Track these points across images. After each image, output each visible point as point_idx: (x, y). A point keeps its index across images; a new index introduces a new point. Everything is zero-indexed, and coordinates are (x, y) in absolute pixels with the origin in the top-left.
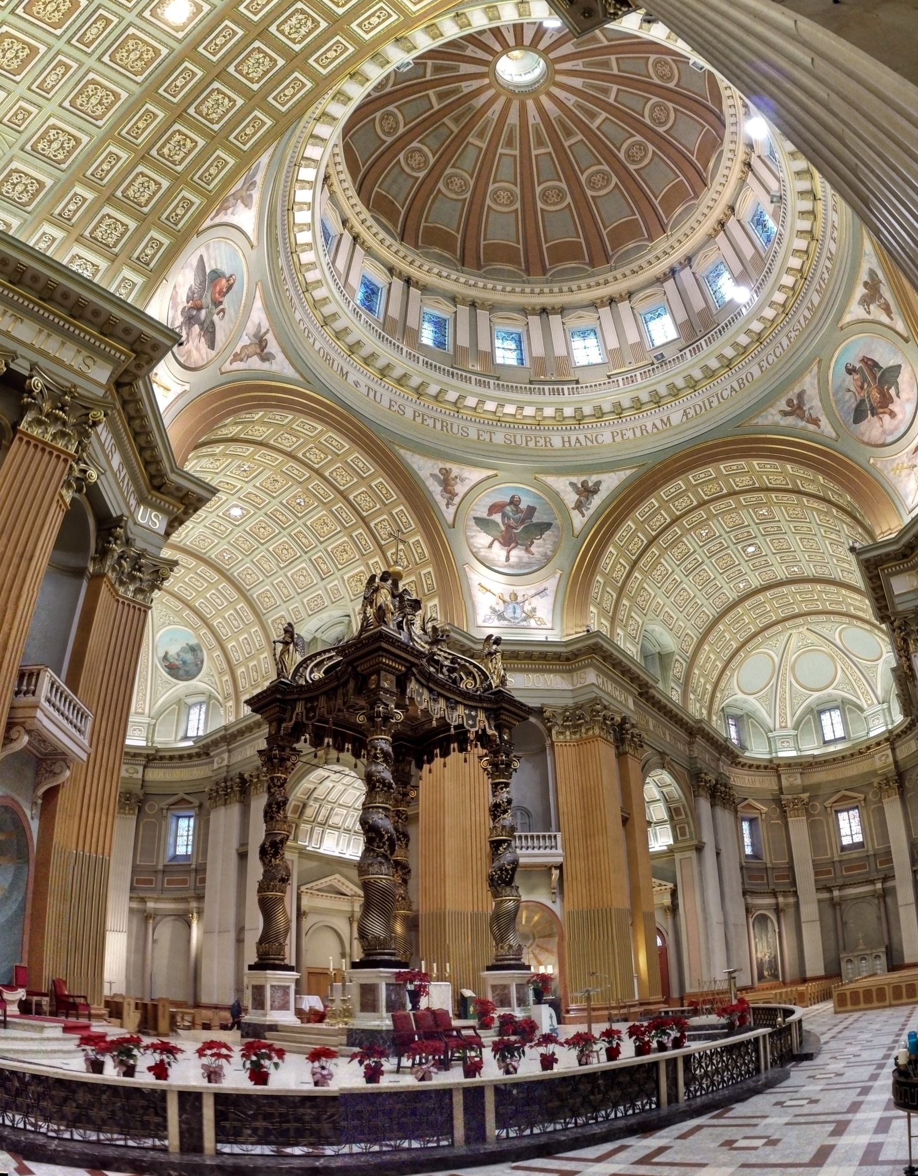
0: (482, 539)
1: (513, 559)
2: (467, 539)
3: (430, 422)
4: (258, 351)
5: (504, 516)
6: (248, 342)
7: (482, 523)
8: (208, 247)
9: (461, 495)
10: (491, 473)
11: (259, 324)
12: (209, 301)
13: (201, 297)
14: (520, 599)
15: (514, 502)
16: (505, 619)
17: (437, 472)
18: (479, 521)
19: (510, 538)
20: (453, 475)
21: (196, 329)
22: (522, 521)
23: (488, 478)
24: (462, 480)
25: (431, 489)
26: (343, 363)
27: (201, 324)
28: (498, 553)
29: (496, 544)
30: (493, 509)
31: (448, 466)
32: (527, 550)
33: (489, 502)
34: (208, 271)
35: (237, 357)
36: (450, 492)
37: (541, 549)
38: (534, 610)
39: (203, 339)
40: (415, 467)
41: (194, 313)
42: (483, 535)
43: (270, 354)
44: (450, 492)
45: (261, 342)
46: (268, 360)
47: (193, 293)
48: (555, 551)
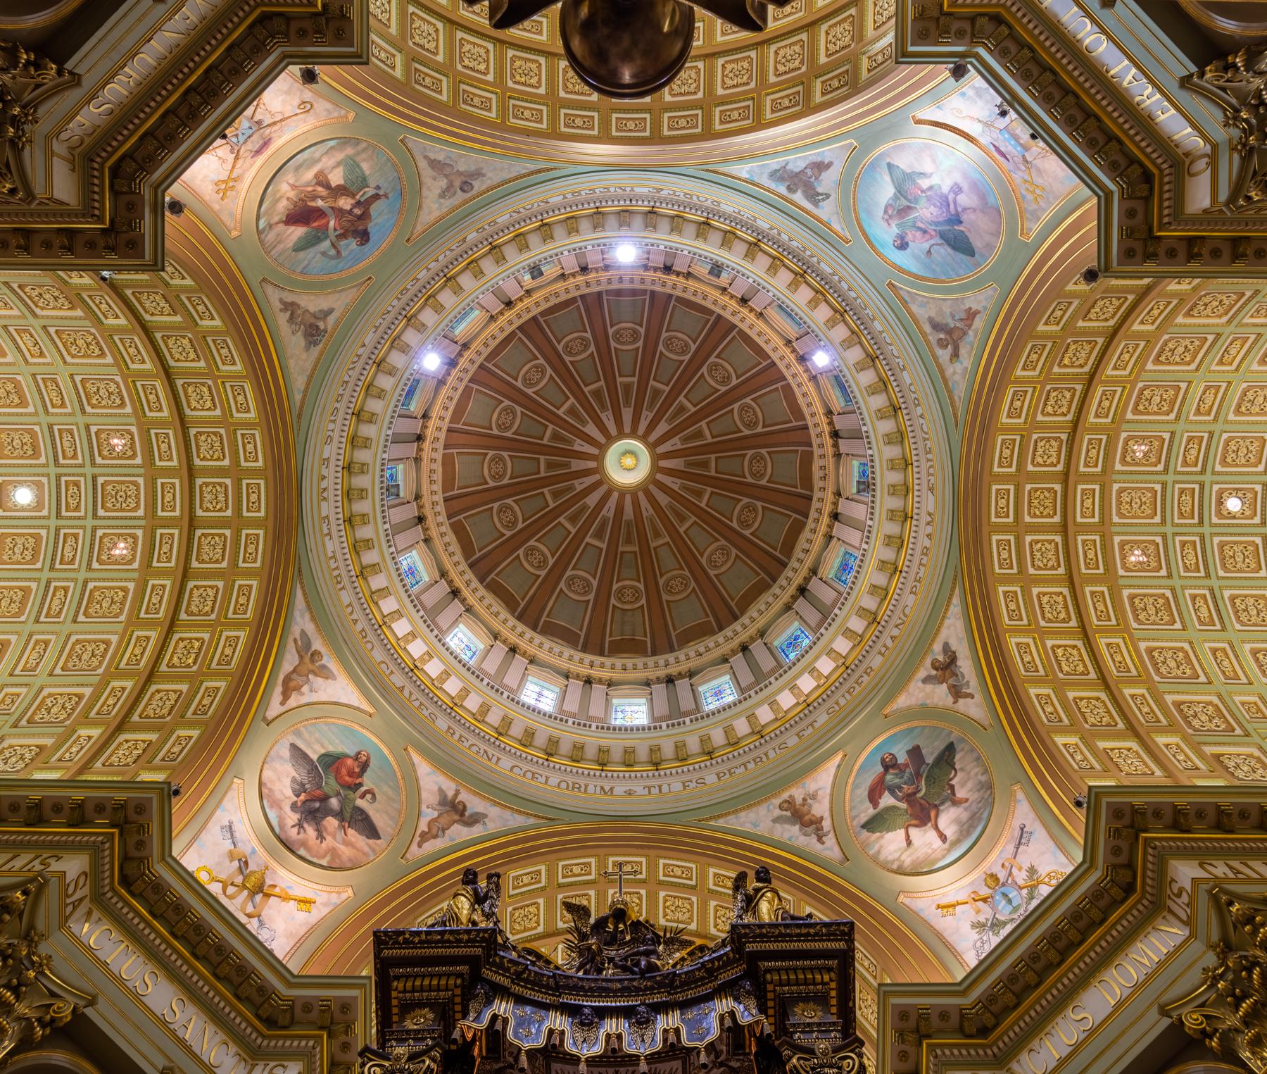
0: (891, 843)
1: (950, 832)
2: (875, 859)
5: (892, 791)
6: (436, 814)
7: (875, 824)
8: (298, 734)
9: (827, 815)
12: (338, 787)
13: (319, 786)
14: (1002, 875)
15: (889, 764)
16: (1004, 924)
17: (777, 812)
18: (871, 825)
19: (922, 808)
20: (799, 800)
21: (331, 823)
22: (918, 775)
24: (814, 796)
26: (599, 783)
27: (339, 815)
28: (925, 839)
29: (913, 831)
30: (874, 796)
32: (956, 803)
33: (863, 792)
34: (314, 757)
37: (970, 785)
38: (1032, 871)
39: (351, 831)
41: (317, 805)
42: (889, 836)
44: (811, 823)
48: (986, 771)
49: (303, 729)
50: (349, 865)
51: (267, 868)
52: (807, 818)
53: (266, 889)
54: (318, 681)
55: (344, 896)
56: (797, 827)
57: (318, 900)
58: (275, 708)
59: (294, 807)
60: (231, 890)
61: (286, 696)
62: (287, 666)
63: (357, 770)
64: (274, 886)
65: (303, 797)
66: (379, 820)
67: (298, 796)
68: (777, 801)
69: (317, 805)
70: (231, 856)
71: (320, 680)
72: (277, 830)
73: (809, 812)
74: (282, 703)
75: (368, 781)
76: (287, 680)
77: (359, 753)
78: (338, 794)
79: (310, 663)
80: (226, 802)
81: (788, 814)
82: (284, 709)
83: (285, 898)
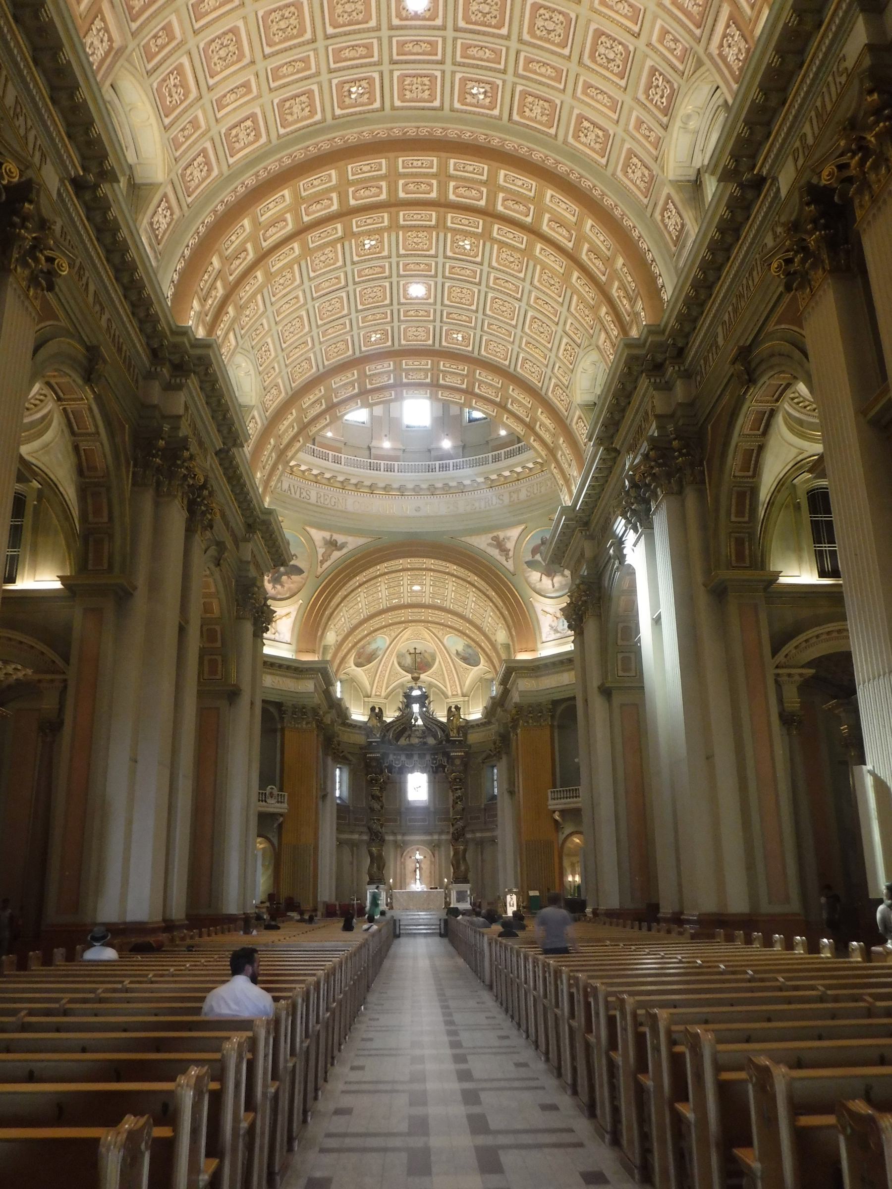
0: (535, 576)
1: (556, 585)
7: (531, 564)
9: (512, 549)
11: (324, 538)
16: (558, 632)
17: (490, 541)
20: (501, 538)
21: (284, 578)
23: (523, 530)
24: (509, 539)
27: (286, 574)
28: (546, 582)
29: (544, 577)
32: (563, 575)
33: (531, 547)
35: (322, 562)
36: (505, 551)
39: (293, 577)
40: (475, 544)
42: (534, 573)
44: (505, 551)
45: (332, 545)
56: (498, 551)
68: (491, 535)
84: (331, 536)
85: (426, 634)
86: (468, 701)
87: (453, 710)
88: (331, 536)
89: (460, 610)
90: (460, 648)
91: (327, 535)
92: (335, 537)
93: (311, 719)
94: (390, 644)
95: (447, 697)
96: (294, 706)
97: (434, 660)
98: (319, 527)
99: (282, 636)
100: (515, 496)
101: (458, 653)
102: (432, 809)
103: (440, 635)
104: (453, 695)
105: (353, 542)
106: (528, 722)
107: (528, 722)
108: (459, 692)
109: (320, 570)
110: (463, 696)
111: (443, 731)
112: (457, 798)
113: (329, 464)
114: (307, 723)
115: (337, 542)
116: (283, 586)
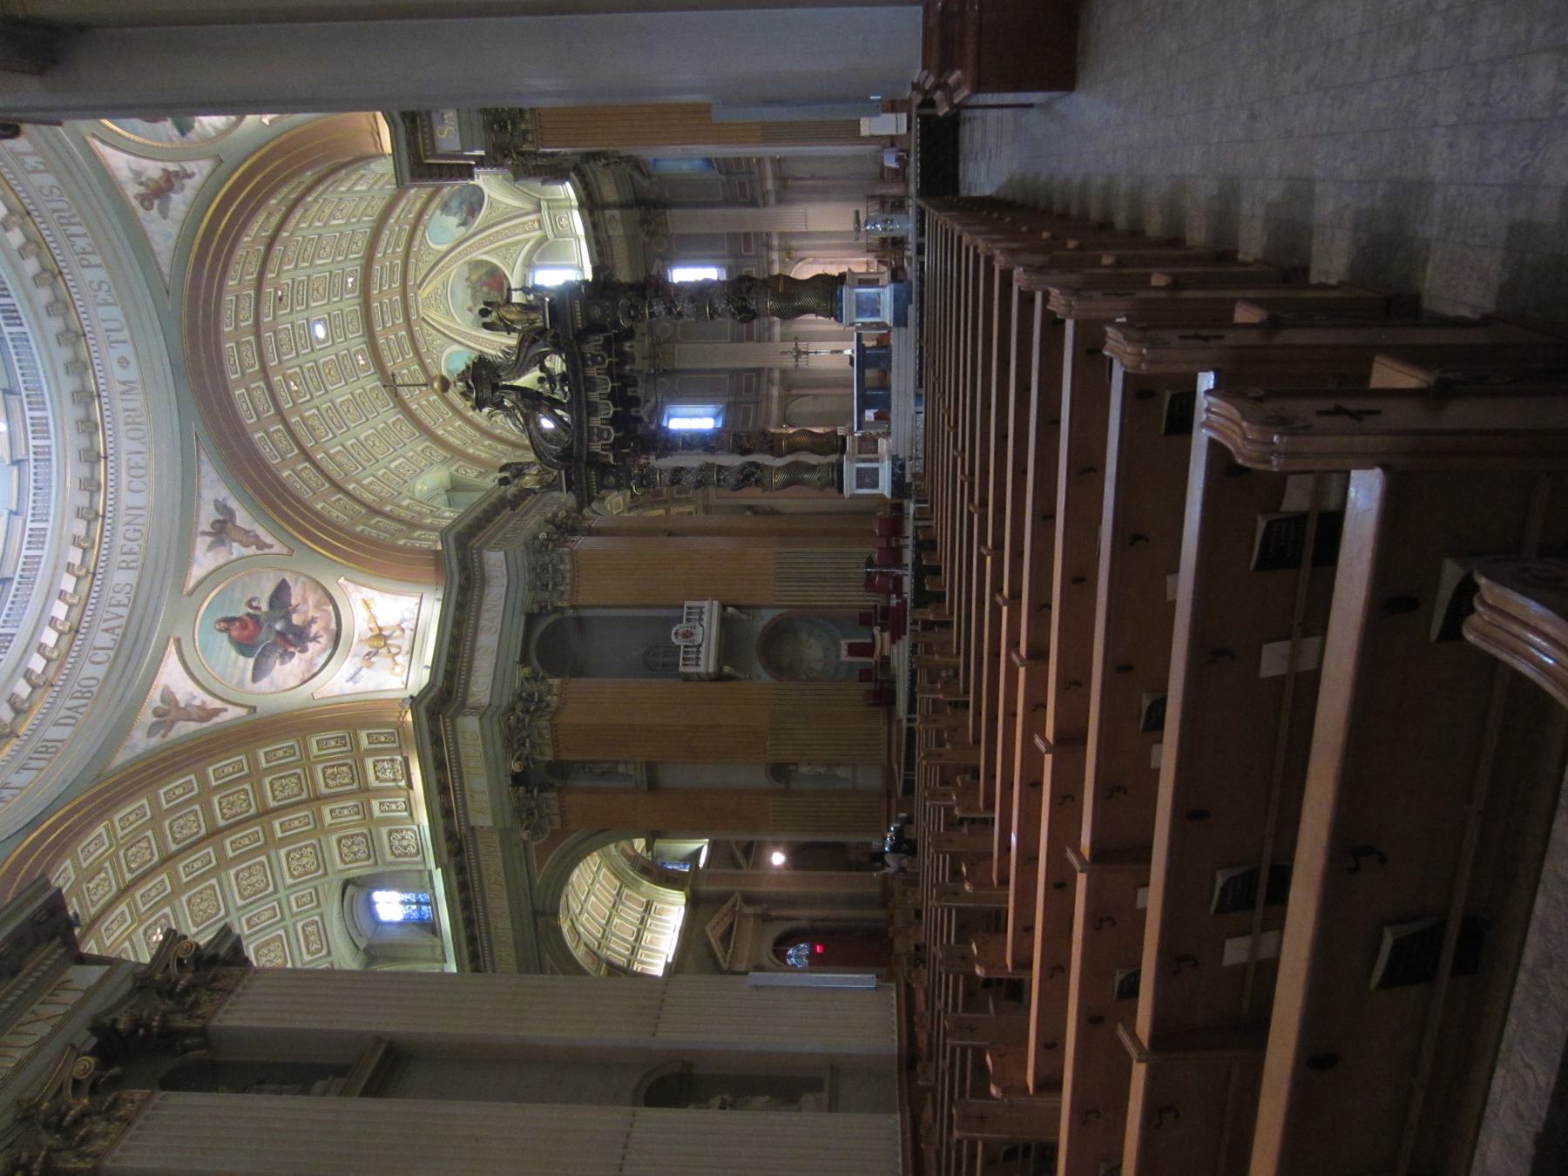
3: (81, 243)
4: (230, 526)
8: (241, 683)
9: (161, 165)
10: (97, 144)
11: (211, 547)
13: (274, 644)
17: (155, 212)
20: (142, 190)
21: (296, 619)
23: (103, 142)
24: (137, 174)
25: (183, 208)
27: (287, 617)
31: (135, 203)
34: (251, 661)
35: (261, 545)
39: (294, 602)
40: (171, 243)
41: (290, 636)
43: (217, 509)
46: (225, 507)
47: (282, 656)
49: (234, 682)
50: (320, 591)
51: (360, 641)
52: (163, 184)
53: (377, 632)
54: (182, 699)
55: (346, 583)
57: (359, 597)
58: (233, 713)
59: (304, 650)
60: (394, 650)
61: (216, 712)
62: (192, 727)
63: (238, 624)
64: (371, 629)
65: (292, 649)
66: (268, 588)
67: (293, 654)
68: (141, 212)
69: (290, 636)
70: (370, 665)
71: (178, 697)
72: (329, 651)
73: (156, 182)
74: (225, 710)
75: (242, 610)
76: (202, 720)
77: (220, 630)
78: (270, 627)
79: (170, 711)
80: (337, 692)
81: (156, 202)
82: (229, 707)
83: (374, 618)
84: (204, 533)
85: (424, 293)
86: (548, 201)
87: (488, 320)
88: (204, 533)
89: (361, 242)
90: (452, 221)
91: (202, 543)
92: (205, 525)
93: (554, 555)
94: (459, 342)
95: (545, 239)
96: (532, 587)
97: (481, 262)
98: (185, 559)
99: (407, 615)
100: (31, 161)
101: (464, 224)
102: (730, 261)
103: (431, 259)
104: (541, 227)
105: (214, 489)
106: (525, 133)
107: (525, 133)
108: (533, 217)
109: (278, 548)
110: (539, 209)
111: (535, 341)
112: (670, 312)
113: (46, 554)
114: (562, 562)
115: (218, 521)
116: (313, 620)
